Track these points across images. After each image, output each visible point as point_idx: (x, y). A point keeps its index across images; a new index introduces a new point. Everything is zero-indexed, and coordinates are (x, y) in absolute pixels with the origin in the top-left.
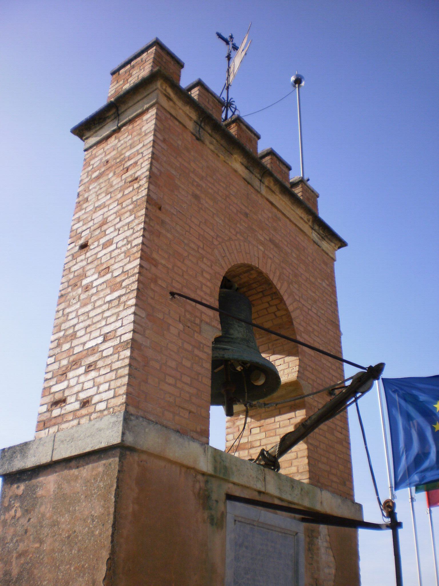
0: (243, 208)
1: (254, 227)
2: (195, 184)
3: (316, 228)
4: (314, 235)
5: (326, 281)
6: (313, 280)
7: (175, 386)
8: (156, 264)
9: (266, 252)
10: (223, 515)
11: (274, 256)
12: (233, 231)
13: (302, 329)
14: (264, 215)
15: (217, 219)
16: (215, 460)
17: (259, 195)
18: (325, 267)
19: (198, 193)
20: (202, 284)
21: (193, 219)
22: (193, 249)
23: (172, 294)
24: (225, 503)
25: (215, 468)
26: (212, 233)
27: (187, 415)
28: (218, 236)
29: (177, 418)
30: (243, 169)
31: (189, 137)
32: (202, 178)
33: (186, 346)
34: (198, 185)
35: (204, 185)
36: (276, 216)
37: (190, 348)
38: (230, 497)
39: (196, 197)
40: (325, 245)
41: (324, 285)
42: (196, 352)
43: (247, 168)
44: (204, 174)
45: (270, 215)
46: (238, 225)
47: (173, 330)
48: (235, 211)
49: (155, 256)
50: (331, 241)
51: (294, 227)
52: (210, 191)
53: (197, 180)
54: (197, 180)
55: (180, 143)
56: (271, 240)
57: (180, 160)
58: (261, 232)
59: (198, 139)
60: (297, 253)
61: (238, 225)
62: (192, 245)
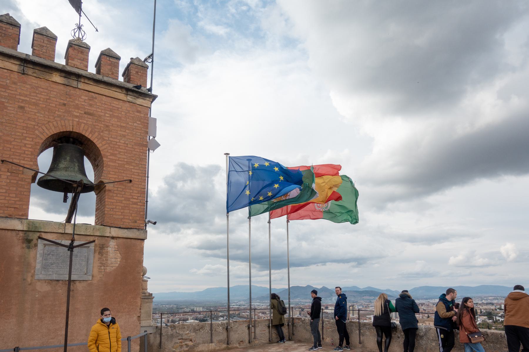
0: (62, 101)
1: (70, 110)
2: (21, 101)
4: (128, 98)
6: (124, 125)
7: (5, 199)
9: (80, 121)
11: (87, 121)
12: (52, 118)
14: (81, 100)
16: (29, 224)
17: (77, 90)
18: (138, 114)
19: (22, 105)
20: (25, 151)
22: (19, 136)
23: (3, 161)
24: (37, 240)
25: (29, 228)
26: (34, 123)
27: (13, 209)
28: (38, 123)
29: (6, 212)
30: (62, 79)
31: (15, 76)
32: (26, 96)
33: (12, 181)
34: (23, 100)
35: (28, 99)
38: (40, 238)
39: (22, 108)
40: (140, 101)
41: (135, 124)
42: (20, 182)
44: (28, 93)
45: (87, 98)
48: (54, 105)
51: (110, 98)
52: (33, 101)
53: (22, 98)
54: (22, 98)
55: (8, 82)
56: (85, 113)
57: (8, 91)
58: (77, 111)
59: (24, 74)
60: (111, 113)
61: (57, 113)
62: (18, 134)
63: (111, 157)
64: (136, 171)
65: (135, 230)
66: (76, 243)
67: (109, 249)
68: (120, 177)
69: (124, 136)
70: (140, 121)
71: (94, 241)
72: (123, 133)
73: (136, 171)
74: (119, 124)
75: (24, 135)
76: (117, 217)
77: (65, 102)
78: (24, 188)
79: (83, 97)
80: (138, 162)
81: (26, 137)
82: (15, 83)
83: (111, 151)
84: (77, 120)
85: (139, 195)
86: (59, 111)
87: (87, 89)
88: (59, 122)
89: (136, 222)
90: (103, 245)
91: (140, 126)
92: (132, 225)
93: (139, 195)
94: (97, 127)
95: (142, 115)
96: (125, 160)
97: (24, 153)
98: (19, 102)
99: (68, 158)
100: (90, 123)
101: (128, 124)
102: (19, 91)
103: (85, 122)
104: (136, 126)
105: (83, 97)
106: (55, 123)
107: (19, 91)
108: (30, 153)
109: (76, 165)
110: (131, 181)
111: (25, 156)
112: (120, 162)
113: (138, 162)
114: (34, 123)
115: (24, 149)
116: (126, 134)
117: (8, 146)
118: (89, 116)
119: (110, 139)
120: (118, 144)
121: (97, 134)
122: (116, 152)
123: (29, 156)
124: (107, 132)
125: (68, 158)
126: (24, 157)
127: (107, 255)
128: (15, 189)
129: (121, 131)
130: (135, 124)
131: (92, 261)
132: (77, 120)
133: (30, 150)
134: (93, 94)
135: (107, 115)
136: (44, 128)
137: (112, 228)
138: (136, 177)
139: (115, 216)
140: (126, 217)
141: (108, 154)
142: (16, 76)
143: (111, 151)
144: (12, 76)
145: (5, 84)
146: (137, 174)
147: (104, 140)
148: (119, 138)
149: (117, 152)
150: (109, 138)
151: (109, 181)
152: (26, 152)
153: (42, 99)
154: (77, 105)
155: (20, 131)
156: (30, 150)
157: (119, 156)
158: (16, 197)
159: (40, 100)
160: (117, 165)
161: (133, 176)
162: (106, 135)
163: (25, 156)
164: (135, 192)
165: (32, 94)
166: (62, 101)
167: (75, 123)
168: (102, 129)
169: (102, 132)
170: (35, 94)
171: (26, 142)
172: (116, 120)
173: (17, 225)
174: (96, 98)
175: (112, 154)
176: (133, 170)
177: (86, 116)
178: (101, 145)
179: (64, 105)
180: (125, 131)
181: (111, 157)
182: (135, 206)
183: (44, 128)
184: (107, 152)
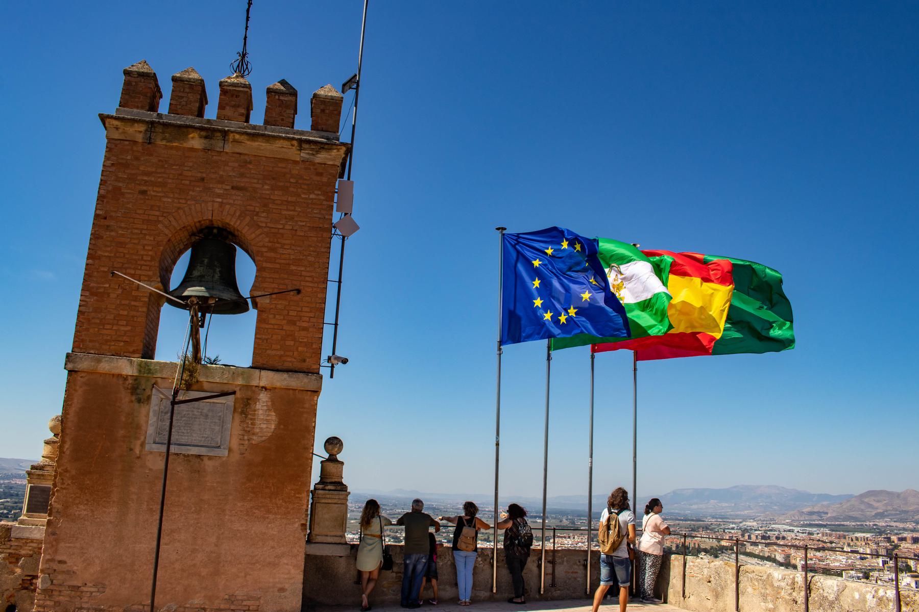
3: (305, 146)
5: (316, 192)
6: (293, 199)
8: (99, 258)
9: (225, 201)
10: (149, 398)
12: (183, 201)
13: (264, 250)
15: (165, 200)
18: (318, 178)
19: (145, 188)
20: (142, 255)
21: (138, 211)
26: (157, 213)
30: (203, 141)
33: (123, 302)
34: (146, 182)
36: (246, 162)
37: (127, 302)
39: (144, 192)
41: (312, 196)
42: (133, 303)
43: (206, 137)
45: (236, 165)
46: (191, 193)
47: (112, 296)
48: (188, 182)
49: (99, 253)
50: (330, 149)
53: (145, 178)
54: (145, 178)
55: (129, 157)
56: (233, 188)
58: (220, 186)
59: (150, 143)
63: (269, 254)
64: (308, 274)
65: (301, 375)
66: (180, 397)
67: (258, 406)
68: (281, 287)
69: (292, 218)
70: (319, 189)
71: (234, 393)
72: (291, 213)
73: (308, 274)
74: (284, 198)
75: (144, 232)
76: (273, 353)
77: (204, 175)
78: (138, 311)
79: (230, 164)
80: (313, 259)
81: (145, 235)
82: (137, 158)
83: (270, 244)
84: (220, 200)
85: (312, 315)
86: (193, 191)
87: (237, 150)
88: (193, 207)
89: (304, 361)
90: (248, 399)
91: (322, 198)
92: (298, 365)
93: (312, 315)
94: (248, 207)
95: (325, 179)
96: (292, 257)
97: (142, 259)
98: (139, 185)
99: (206, 261)
100: (239, 202)
101: (299, 196)
102: (142, 168)
103: (231, 201)
104: (312, 199)
105: (230, 164)
106: (186, 209)
107: (142, 168)
108: (149, 258)
109: (218, 270)
110: (299, 291)
111: (143, 262)
112: (283, 261)
113: (313, 259)
114: (157, 213)
115: (142, 253)
116: (296, 213)
117: (121, 250)
118: (238, 193)
119: (269, 225)
120: (281, 231)
121: (248, 219)
122: (277, 245)
123: (148, 263)
124: (264, 214)
125: (206, 261)
126: (141, 265)
127: (254, 415)
128: (125, 313)
129: (287, 210)
130: (312, 196)
131: (229, 426)
132: (220, 200)
133: (150, 253)
134: (246, 157)
135: (266, 187)
136: (172, 219)
137: (263, 372)
138: (307, 284)
139: (269, 352)
140: (288, 353)
141: (264, 250)
142: (140, 148)
143: (270, 244)
144: (135, 148)
145: (124, 162)
146: (310, 279)
147: (259, 227)
148: (283, 222)
149: (279, 245)
150: (266, 223)
151: (263, 293)
152: (145, 258)
153: (171, 176)
154: (221, 176)
155: (139, 226)
156: (150, 253)
157: (281, 251)
158: (127, 325)
159: (169, 178)
160: (278, 266)
161: (303, 283)
162: (262, 219)
163: (143, 262)
164: (305, 309)
165: (159, 171)
166: (199, 175)
167: (216, 205)
168: (257, 209)
169: (257, 214)
170: (163, 170)
171: (145, 242)
172: (280, 193)
173: (127, 367)
174: (250, 163)
175: (272, 250)
176: (303, 273)
177: (234, 192)
178: (253, 236)
179: (203, 179)
180: (294, 210)
181: (269, 254)
182: (303, 333)
183: (172, 219)
184: (264, 246)
